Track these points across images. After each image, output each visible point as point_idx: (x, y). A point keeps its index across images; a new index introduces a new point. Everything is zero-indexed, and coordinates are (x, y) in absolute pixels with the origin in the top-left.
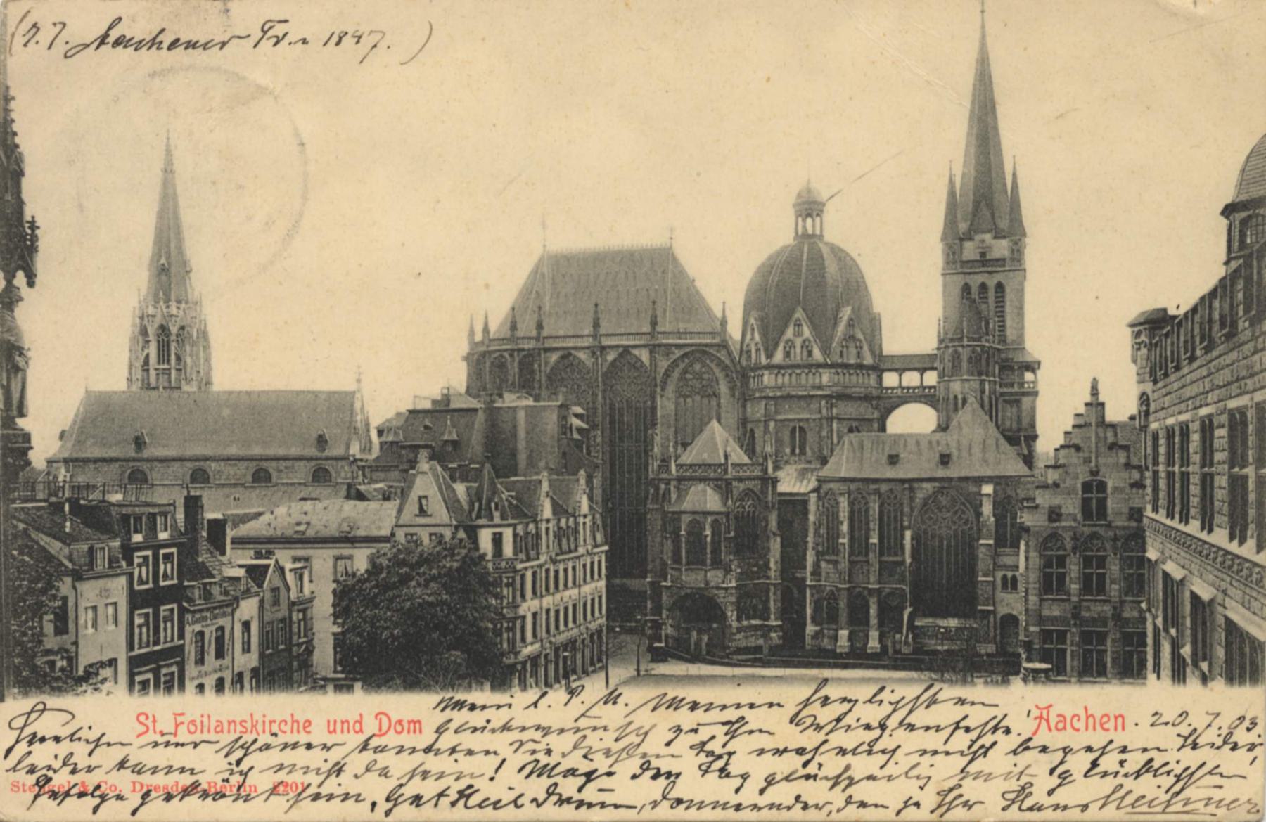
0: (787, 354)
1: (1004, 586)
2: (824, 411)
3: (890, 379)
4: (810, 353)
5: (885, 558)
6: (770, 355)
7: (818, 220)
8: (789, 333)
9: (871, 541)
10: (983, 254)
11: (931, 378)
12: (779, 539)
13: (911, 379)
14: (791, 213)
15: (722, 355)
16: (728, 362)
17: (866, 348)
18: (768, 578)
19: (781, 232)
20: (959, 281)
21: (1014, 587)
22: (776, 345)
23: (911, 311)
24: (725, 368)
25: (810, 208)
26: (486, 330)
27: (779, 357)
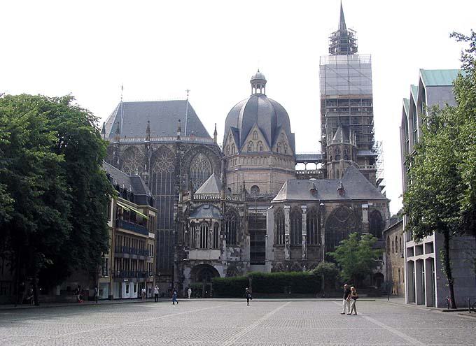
0: (249, 149)
3: (300, 167)
7: (263, 89)
8: (249, 138)
11: (320, 166)
13: (311, 167)
23: (308, 135)
25: (259, 82)
27: (245, 150)
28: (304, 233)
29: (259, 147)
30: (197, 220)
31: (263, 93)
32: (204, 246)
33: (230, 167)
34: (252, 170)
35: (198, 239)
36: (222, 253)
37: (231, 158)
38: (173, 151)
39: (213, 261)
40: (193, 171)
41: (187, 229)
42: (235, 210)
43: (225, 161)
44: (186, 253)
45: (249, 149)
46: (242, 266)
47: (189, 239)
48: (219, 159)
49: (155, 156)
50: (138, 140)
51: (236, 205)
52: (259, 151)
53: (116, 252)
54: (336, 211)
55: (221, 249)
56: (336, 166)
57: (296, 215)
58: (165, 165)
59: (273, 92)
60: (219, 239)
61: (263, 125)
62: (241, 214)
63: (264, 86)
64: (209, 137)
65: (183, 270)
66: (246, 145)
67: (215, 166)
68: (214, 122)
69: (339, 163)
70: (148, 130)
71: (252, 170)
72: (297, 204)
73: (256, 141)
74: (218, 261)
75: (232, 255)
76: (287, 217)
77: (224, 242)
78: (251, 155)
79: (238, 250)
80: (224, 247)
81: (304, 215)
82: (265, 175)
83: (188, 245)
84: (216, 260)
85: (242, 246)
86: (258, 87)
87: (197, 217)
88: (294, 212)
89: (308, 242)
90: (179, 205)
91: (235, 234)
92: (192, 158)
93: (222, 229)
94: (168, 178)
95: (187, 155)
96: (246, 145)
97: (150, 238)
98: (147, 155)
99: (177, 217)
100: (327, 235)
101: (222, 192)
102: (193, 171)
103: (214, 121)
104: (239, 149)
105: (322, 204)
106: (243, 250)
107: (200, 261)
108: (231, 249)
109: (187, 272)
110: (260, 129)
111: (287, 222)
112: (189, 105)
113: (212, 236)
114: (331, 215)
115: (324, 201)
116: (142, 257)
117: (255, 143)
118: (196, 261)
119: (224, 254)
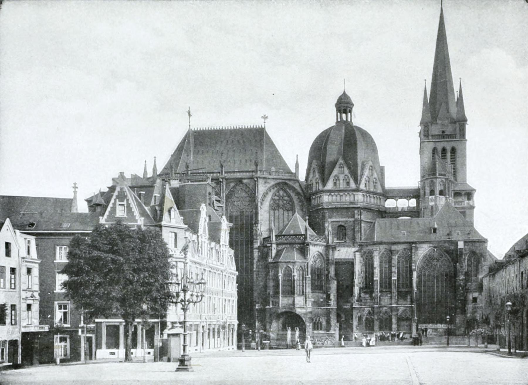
0: (335, 184)
2: (356, 216)
4: (348, 183)
5: (400, 290)
6: (324, 185)
7: (349, 114)
8: (335, 172)
9: (393, 278)
10: (443, 132)
11: (413, 203)
12: (336, 282)
14: (334, 110)
15: (296, 186)
16: (299, 190)
18: (329, 305)
19: (329, 119)
20: (430, 146)
22: (328, 179)
24: (298, 194)
26: (155, 170)
27: (330, 185)
31: (349, 120)
37: (313, 194)
59: (359, 119)
63: (350, 112)
86: (345, 112)
103: (295, 154)
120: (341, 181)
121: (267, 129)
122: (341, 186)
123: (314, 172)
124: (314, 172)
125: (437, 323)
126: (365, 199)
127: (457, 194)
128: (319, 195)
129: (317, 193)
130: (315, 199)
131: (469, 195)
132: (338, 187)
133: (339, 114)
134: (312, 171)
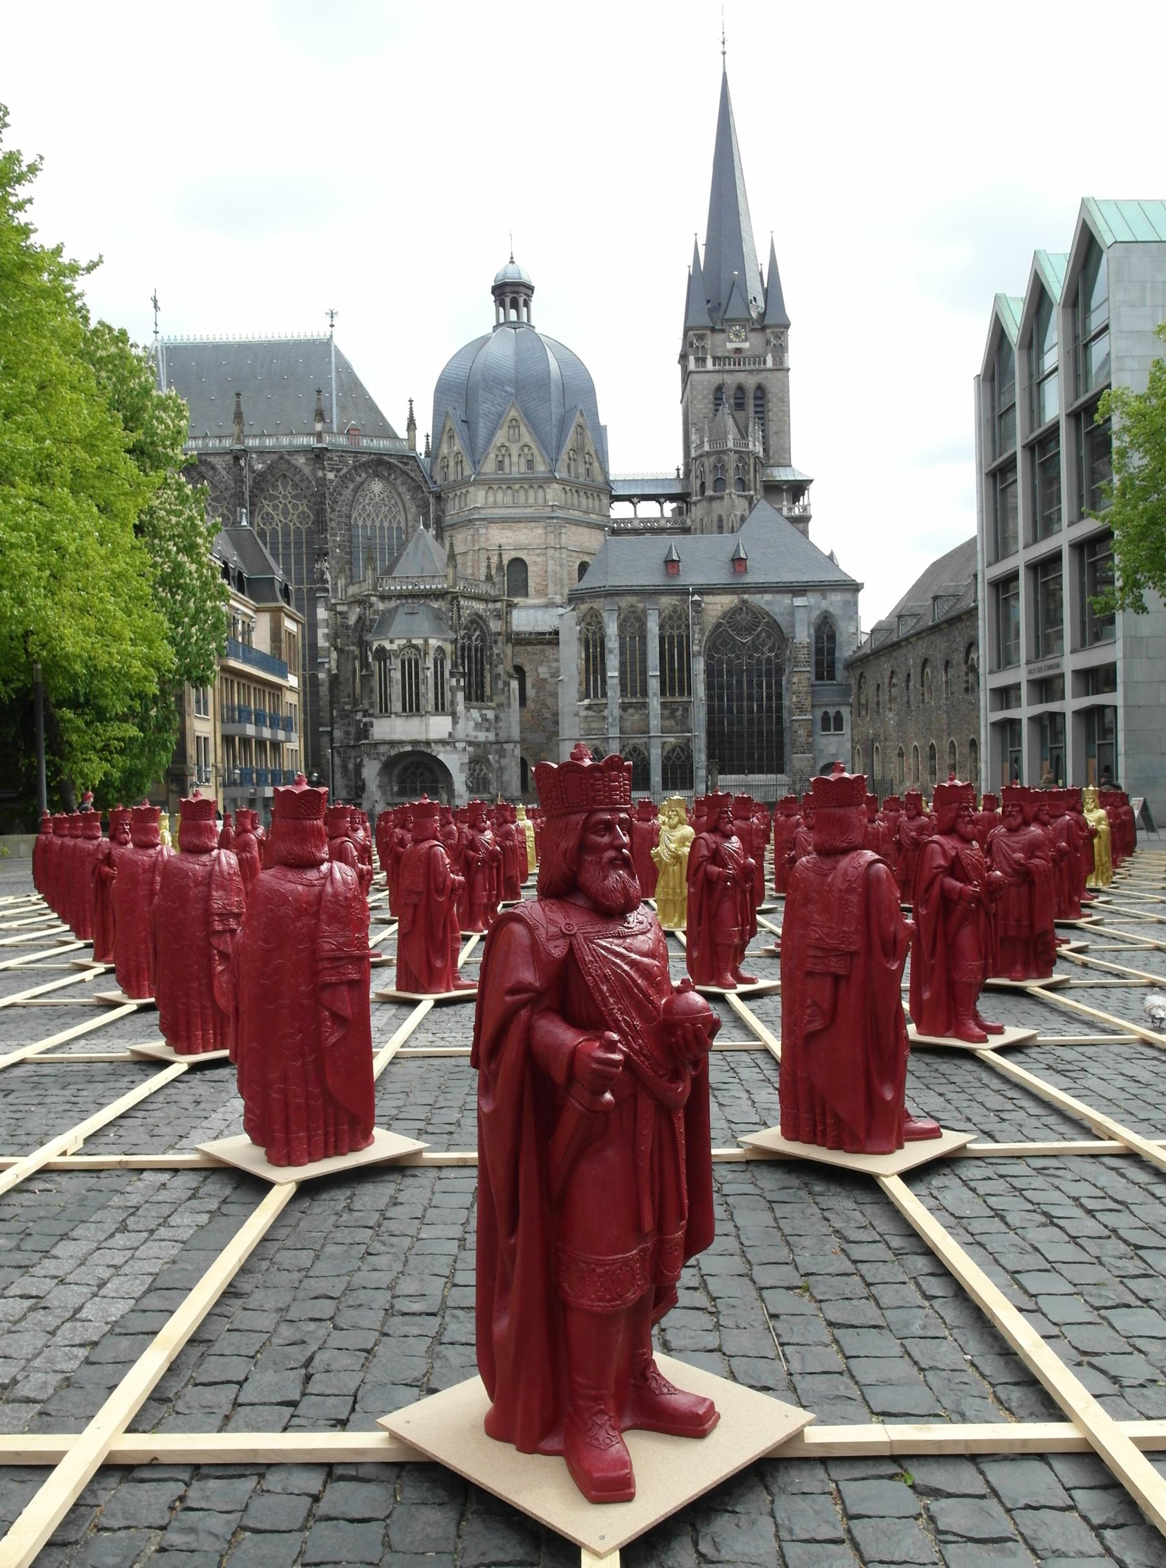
1: (826, 727)
3: (621, 511)
4: (530, 464)
8: (500, 438)
13: (649, 510)
17: (596, 464)
21: (839, 726)
27: (489, 466)
28: (654, 671)
29: (523, 461)
30: (392, 642)
32: (412, 707)
33: (452, 511)
34: (504, 520)
35: (396, 690)
36: (455, 722)
38: (307, 470)
39: (438, 742)
40: (360, 523)
41: (365, 665)
42: (481, 617)
43: (438, 498)
44: (365, 724)
45: (501, 463)
46: (502, 753)
47: (372, 691)
48: (423, 488)
49: (260, 481)
50: (213, 443)
51: (479, 606)
52: (523, 469)
53: (223, 722)
54: (731, 615)
55: (454, 714)
56: (716, 505)
57: (633, 626)
58: (286, 511)
60: (447, 688)
61: (520, 403)
62: (495, 626)
63: (526, 304)
64: (396, 437)
65: (359, 767)
66: (492, 456)
67: (414, 510)
68: (403, 394)
69: (721, 498)
70: (238, 416)
71: (504, 520)
72: (632, 599)
73: (512, 447)
74: (448, 742)
75: (478, 726)
76: (612, 629)
77: (460, 696)
78: (508, 483)
79: (490, 714)
80: (460, 708)
81: (653, 626)
82: (540, 531)
83: (372, 705)
84: (442, 742)
85: (500, 705)
86: (515, 305)
87: (390, 636)
88: (625, 620)
89: (663, 693)
90: (339, 608)
91: (483, 676)
92: (355, 491)
93: (455, 665)
94: (298, 545)
95: (344, 480)
96: (492, 456)
97: (291, 689)
98: (239, 480)
99: (333, 638)
100: (709, 672)
101: (450, 571)
102: (360, 523)
103: (403, 394)
104: (475, 463)
105: (696, 598)
106: (502, 715)
107: (401, 743)
108: (475, 713)
109: (371, 771)
110: (526, 414)
111: (613, 644)
112: (338, 352)
113: (431, 682)
114: (719, 625)
115: (703, 591)
116: (281, 735)
117: (514, 449)
118: (392, 743)
119: (460, 726)
120: (515, 459)
121: (336, 341)
122: (515, 469)
123: (451, 437)
124: (451, 437)
125: (751, 772)
126: (569, 500)
127: (773, 489)
128: (464, 491)
129: (456, 485)
130: (454, 499)
131: (798, 489)
132: (507, 470)
133: (501, 309)
134: (445, 438)
